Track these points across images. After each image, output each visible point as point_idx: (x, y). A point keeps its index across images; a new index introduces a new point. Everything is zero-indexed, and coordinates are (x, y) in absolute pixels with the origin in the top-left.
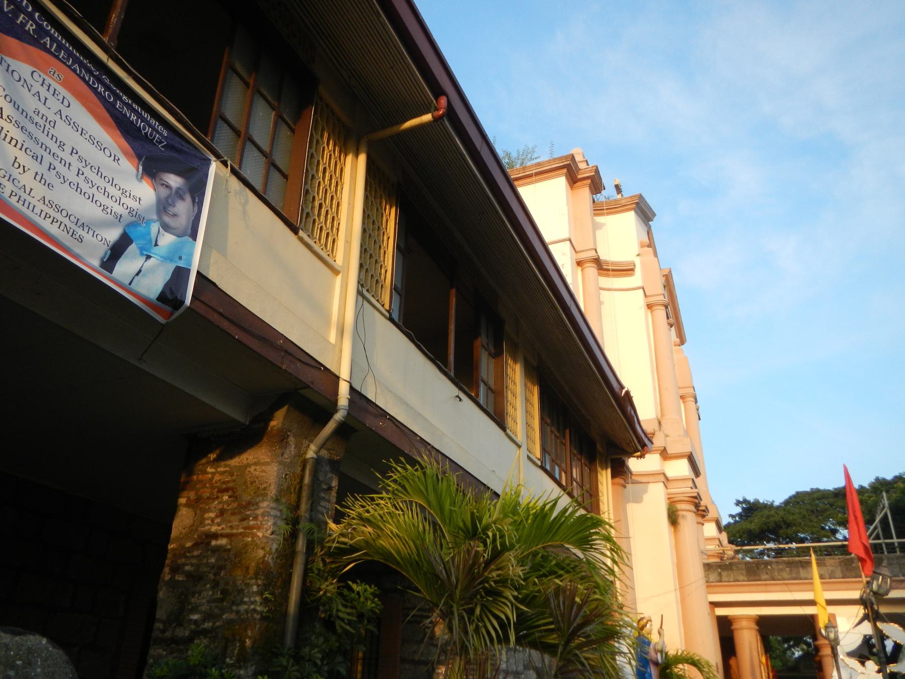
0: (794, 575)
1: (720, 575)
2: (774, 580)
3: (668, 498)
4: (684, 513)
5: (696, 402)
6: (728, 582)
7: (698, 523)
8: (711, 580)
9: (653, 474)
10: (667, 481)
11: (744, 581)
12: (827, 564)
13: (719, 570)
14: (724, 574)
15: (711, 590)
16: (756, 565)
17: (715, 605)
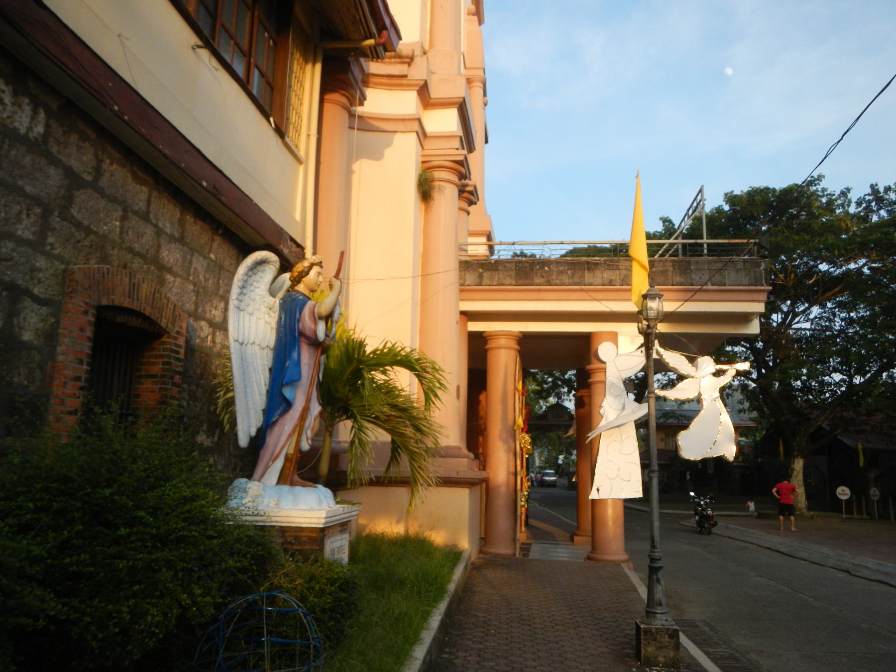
0: (576, 280)
1: (481, 276)
2: (550, 285)
3: (423, 162)
4: (442, 184)
5: (485, 95)
6: (490, 285)
7: (461, 209)
8: (467, 282)
9: (403, 120)
10: (423, 135)
11: (510, 285)
12: (621, 267)
13: (480, 270)
14: (486, 275)
15: (465, 295)
16: (530, 265)
17: (469, 316)
